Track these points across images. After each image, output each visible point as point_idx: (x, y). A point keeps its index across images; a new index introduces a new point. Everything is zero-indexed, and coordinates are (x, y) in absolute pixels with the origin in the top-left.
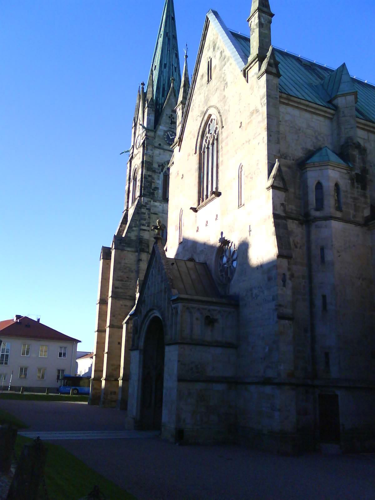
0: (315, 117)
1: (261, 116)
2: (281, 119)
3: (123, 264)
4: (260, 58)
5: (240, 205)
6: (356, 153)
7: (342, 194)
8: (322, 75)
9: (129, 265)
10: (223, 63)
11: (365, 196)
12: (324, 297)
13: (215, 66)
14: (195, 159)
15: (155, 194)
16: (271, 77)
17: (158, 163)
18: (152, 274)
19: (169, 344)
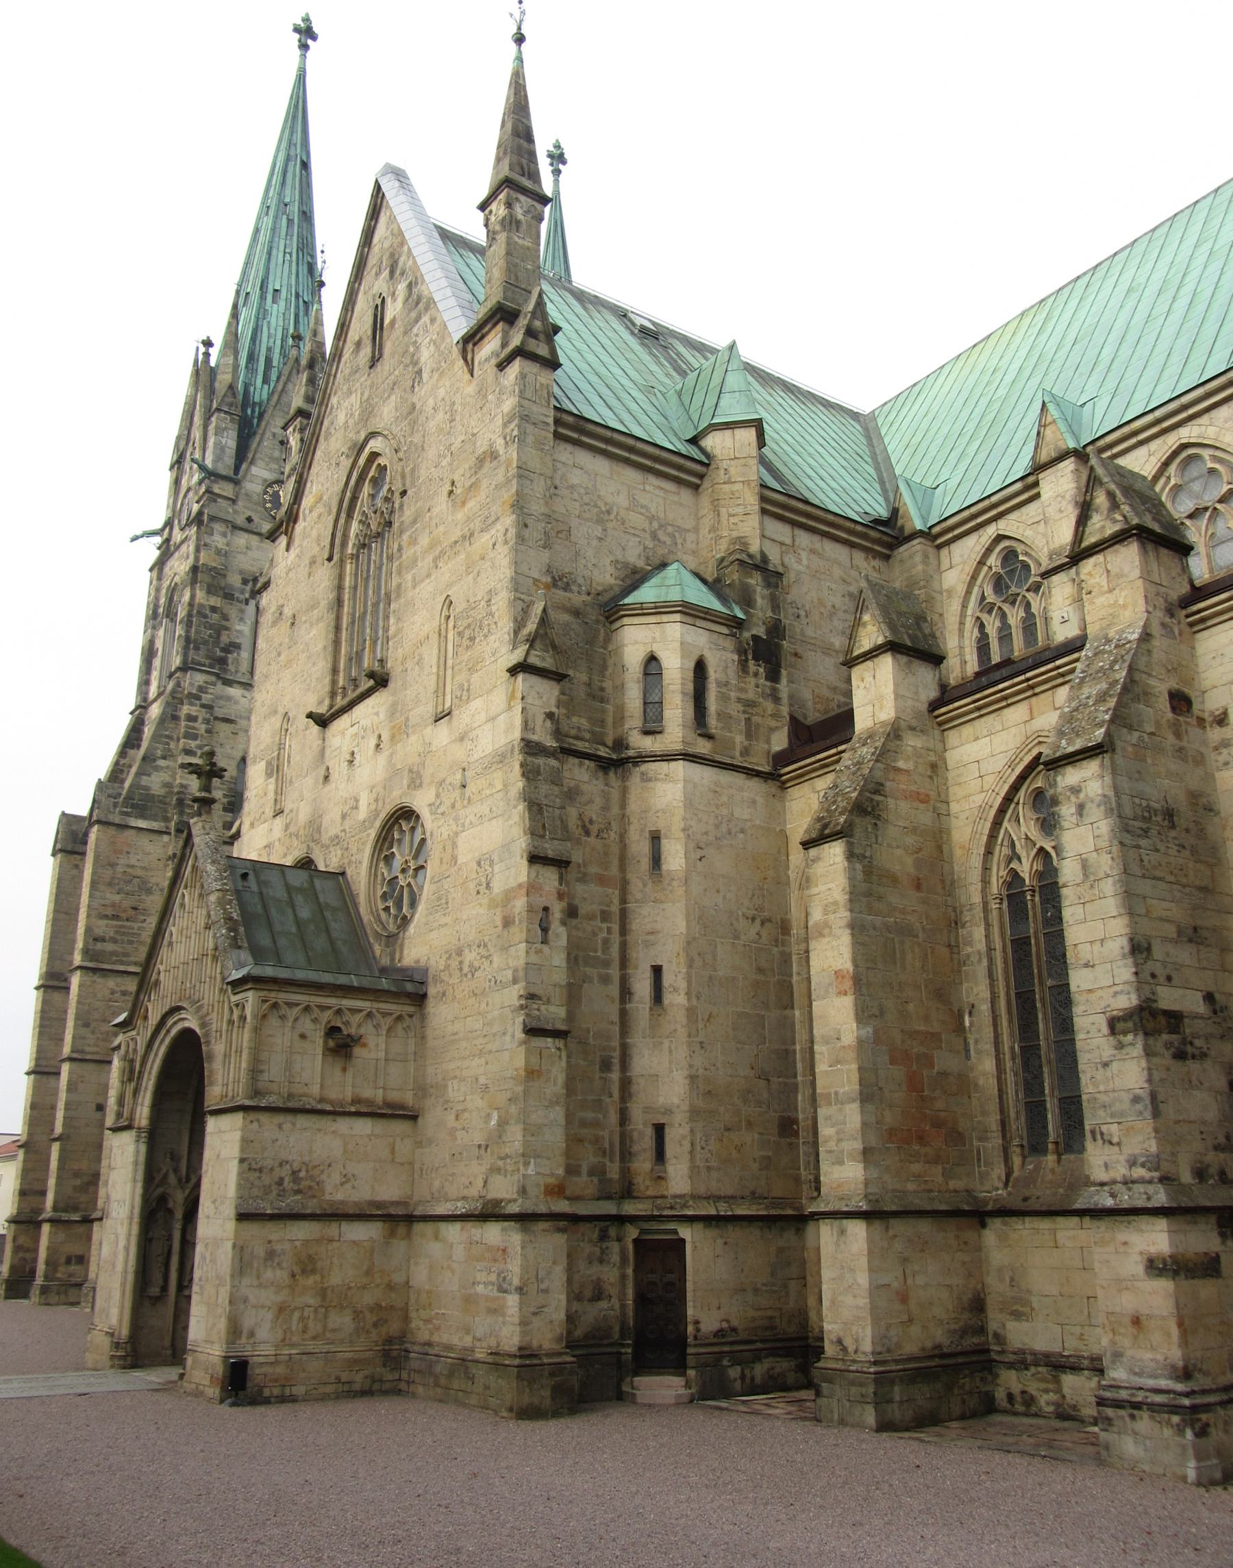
0: (653, 480)
1: (501, 471)
2: (557, 482)
3: (120, 869)
9: (140, 872)
10: (413, 315)
11: (776, 699)
12: (657, 971)
15: (230, 661)
17: (241, 572)
18: (182, 905)
19: (217, 1112)
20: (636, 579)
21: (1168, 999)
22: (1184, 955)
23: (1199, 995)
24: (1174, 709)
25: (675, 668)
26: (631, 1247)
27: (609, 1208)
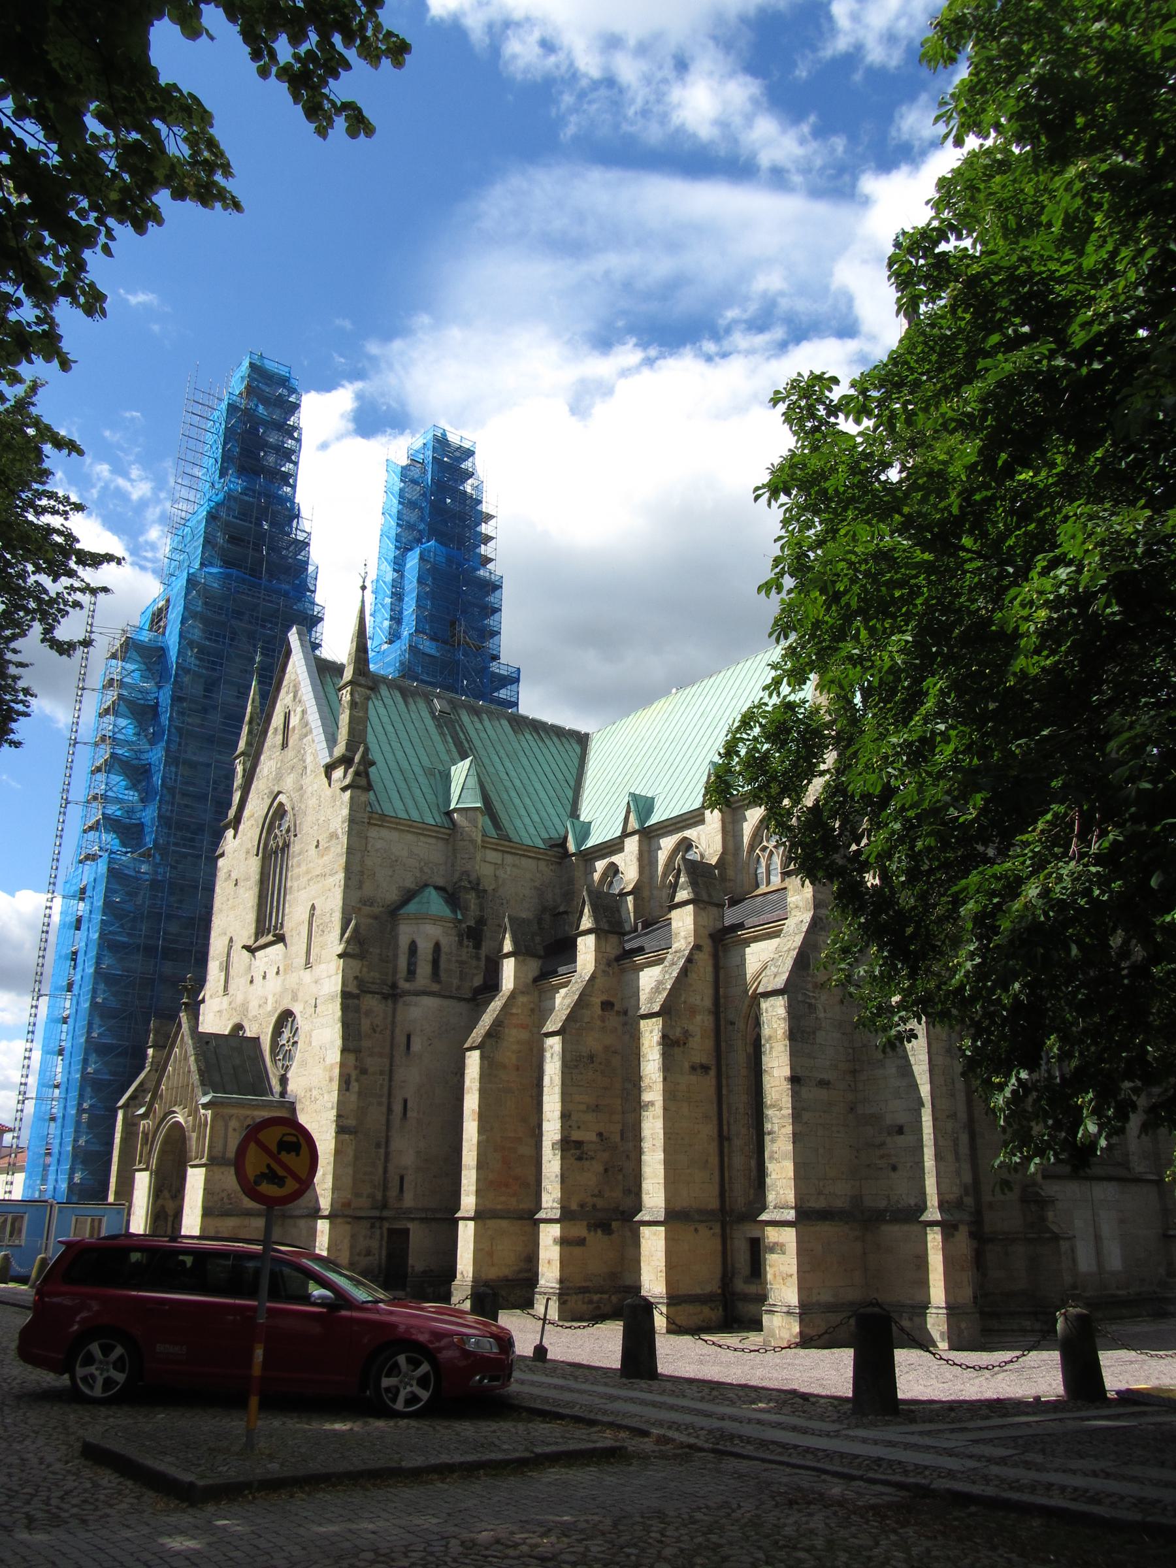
0: (422, 838)
4: (345, 761)
5: (308, 965)
6: (471, 897)
7: (443, 958)
8: (465, 733)
10: (304, 731)
11: (478, 959)
12: (405, 1101)
14: (253, 866)
16: (358, 792)
20: (409, 896)
21: (576, 1136)
23: (594, 1134)
24: (603, 1009)
26: (385, 1234)
27: (376, 1213)
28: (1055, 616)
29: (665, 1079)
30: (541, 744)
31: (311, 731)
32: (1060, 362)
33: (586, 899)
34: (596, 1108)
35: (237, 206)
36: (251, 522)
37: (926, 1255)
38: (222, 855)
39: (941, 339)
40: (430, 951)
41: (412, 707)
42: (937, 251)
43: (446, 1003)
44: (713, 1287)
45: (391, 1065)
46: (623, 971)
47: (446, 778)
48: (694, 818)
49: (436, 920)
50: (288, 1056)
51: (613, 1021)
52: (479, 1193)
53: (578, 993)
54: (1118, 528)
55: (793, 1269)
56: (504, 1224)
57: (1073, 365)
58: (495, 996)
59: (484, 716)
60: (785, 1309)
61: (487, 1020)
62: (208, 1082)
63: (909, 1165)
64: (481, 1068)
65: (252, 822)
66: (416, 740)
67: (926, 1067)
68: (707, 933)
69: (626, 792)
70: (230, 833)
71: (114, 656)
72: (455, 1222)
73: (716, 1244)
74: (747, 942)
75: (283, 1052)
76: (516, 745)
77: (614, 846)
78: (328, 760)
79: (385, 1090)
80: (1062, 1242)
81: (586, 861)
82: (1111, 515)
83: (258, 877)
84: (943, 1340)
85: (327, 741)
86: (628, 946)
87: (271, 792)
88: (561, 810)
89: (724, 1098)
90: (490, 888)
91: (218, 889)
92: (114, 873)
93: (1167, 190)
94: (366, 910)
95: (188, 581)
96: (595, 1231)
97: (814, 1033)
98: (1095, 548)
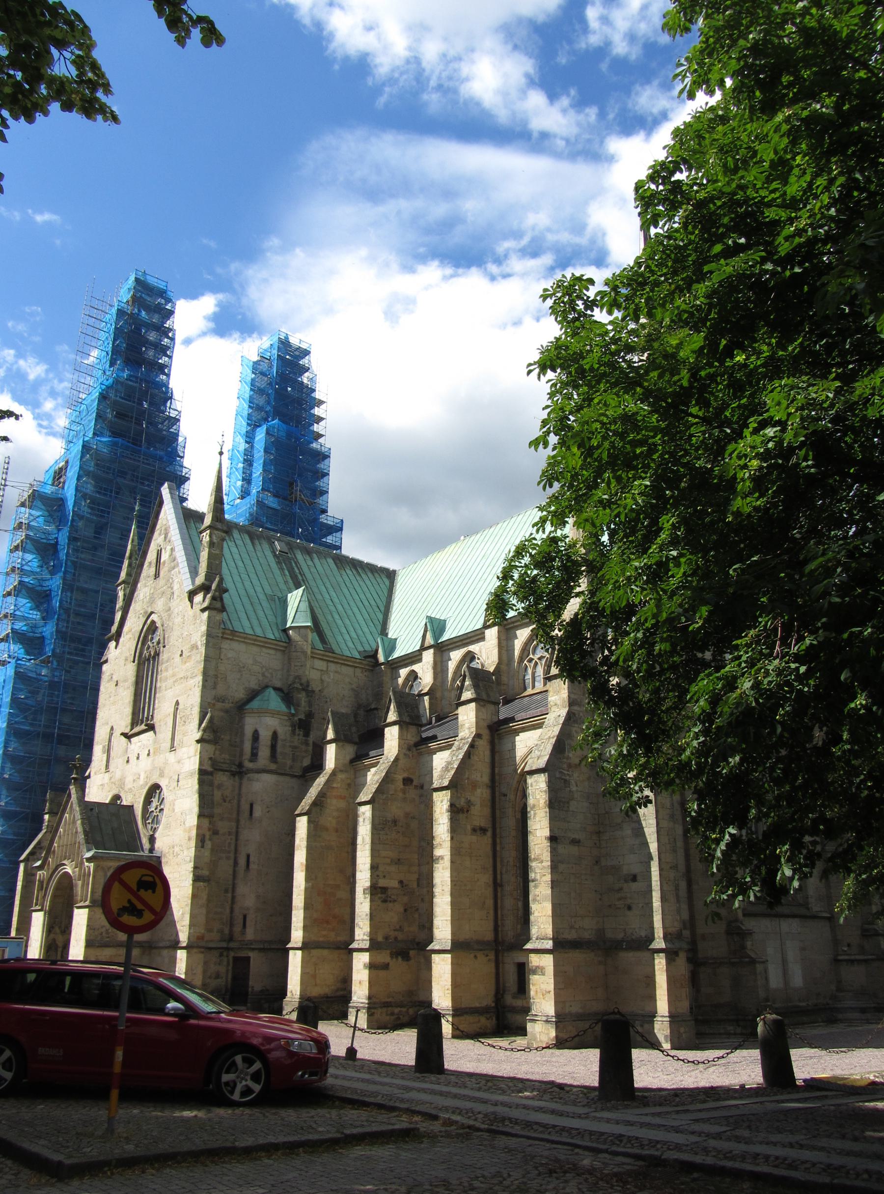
0: (264, 650)
1: (199, 655)
4: (205, 588)
5: (172, 748)
6: (302, 697)
10: (172, 564)
11: (307, 744)
12: (248, 856)
13: (164, 562)
14: (130, 671)
16: (214, 613)
20: (253, 695)
21: (382, 883)
22: (393, 868)
23: (397, 882)
24: (404, 784)
25: (265, 736)
27: (224, 945)
28: (765, 465)
29: (452, 838)
30: (358, 578)
31: (178, 565)
32: (769, 266)
33: (392, 697)
34: (398, 862)
35: (115, 118)
36: (134, 402)
37: (654, 975)
38: (106, 661)
39: (675, 248)
40: (270, 738)
41: (258, 547)
42: (673, 179)
43: (281, 779)
44: (488, 1001)
45: (237, 828)
46: (420, 754)
47: (284, 603)
48: (477, 636)
49: (274, 714)
50: (156, 820)
51: (412, 793)
52: (305, 928)
53: (385, 771)
54: (814, 396)
55: (551, 987)
56: (325, 952)
57: (779, 269)
58: (320, 774)
59: (315, 555)
60: (544, 1019)
61: (313, 792)
62: (91, 839)
63: (641, 905)
64: (308, 830)
65: (130, 636)
66: (260, 573)
67: (654, 829)
68: (485, 724)
69: (424, 615)
70: (112, 644)
71: (23, 505)
72: (287, 951)
73: (490, 968)
74: (517, 732)
75: (151, 817)
76: (340, 579)
77: (414, 658)
78: (191, 587)
79: (233, 847)
80: (758, 965)
81: (393, 669)
82: (808, 386)
83: (134, 679)
84: (667, 1042)
85: (190, 572)
86: (424, 735)
87: (146, 612)
88: (373, 629)
89: (498, 854)
90: (317, 689)
91: (102, 688)
92: (20, 676)
93: (854, 132)
94: (219, 705)
95: (84, 446)
96: (397, 957)
97: (568, 803)
98: (796, 411)
